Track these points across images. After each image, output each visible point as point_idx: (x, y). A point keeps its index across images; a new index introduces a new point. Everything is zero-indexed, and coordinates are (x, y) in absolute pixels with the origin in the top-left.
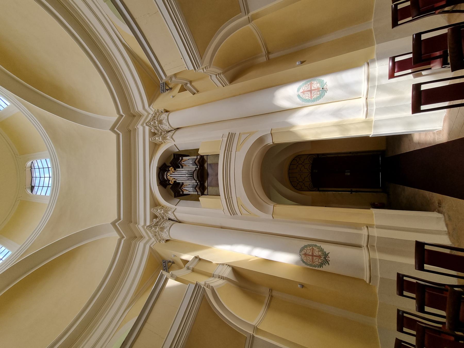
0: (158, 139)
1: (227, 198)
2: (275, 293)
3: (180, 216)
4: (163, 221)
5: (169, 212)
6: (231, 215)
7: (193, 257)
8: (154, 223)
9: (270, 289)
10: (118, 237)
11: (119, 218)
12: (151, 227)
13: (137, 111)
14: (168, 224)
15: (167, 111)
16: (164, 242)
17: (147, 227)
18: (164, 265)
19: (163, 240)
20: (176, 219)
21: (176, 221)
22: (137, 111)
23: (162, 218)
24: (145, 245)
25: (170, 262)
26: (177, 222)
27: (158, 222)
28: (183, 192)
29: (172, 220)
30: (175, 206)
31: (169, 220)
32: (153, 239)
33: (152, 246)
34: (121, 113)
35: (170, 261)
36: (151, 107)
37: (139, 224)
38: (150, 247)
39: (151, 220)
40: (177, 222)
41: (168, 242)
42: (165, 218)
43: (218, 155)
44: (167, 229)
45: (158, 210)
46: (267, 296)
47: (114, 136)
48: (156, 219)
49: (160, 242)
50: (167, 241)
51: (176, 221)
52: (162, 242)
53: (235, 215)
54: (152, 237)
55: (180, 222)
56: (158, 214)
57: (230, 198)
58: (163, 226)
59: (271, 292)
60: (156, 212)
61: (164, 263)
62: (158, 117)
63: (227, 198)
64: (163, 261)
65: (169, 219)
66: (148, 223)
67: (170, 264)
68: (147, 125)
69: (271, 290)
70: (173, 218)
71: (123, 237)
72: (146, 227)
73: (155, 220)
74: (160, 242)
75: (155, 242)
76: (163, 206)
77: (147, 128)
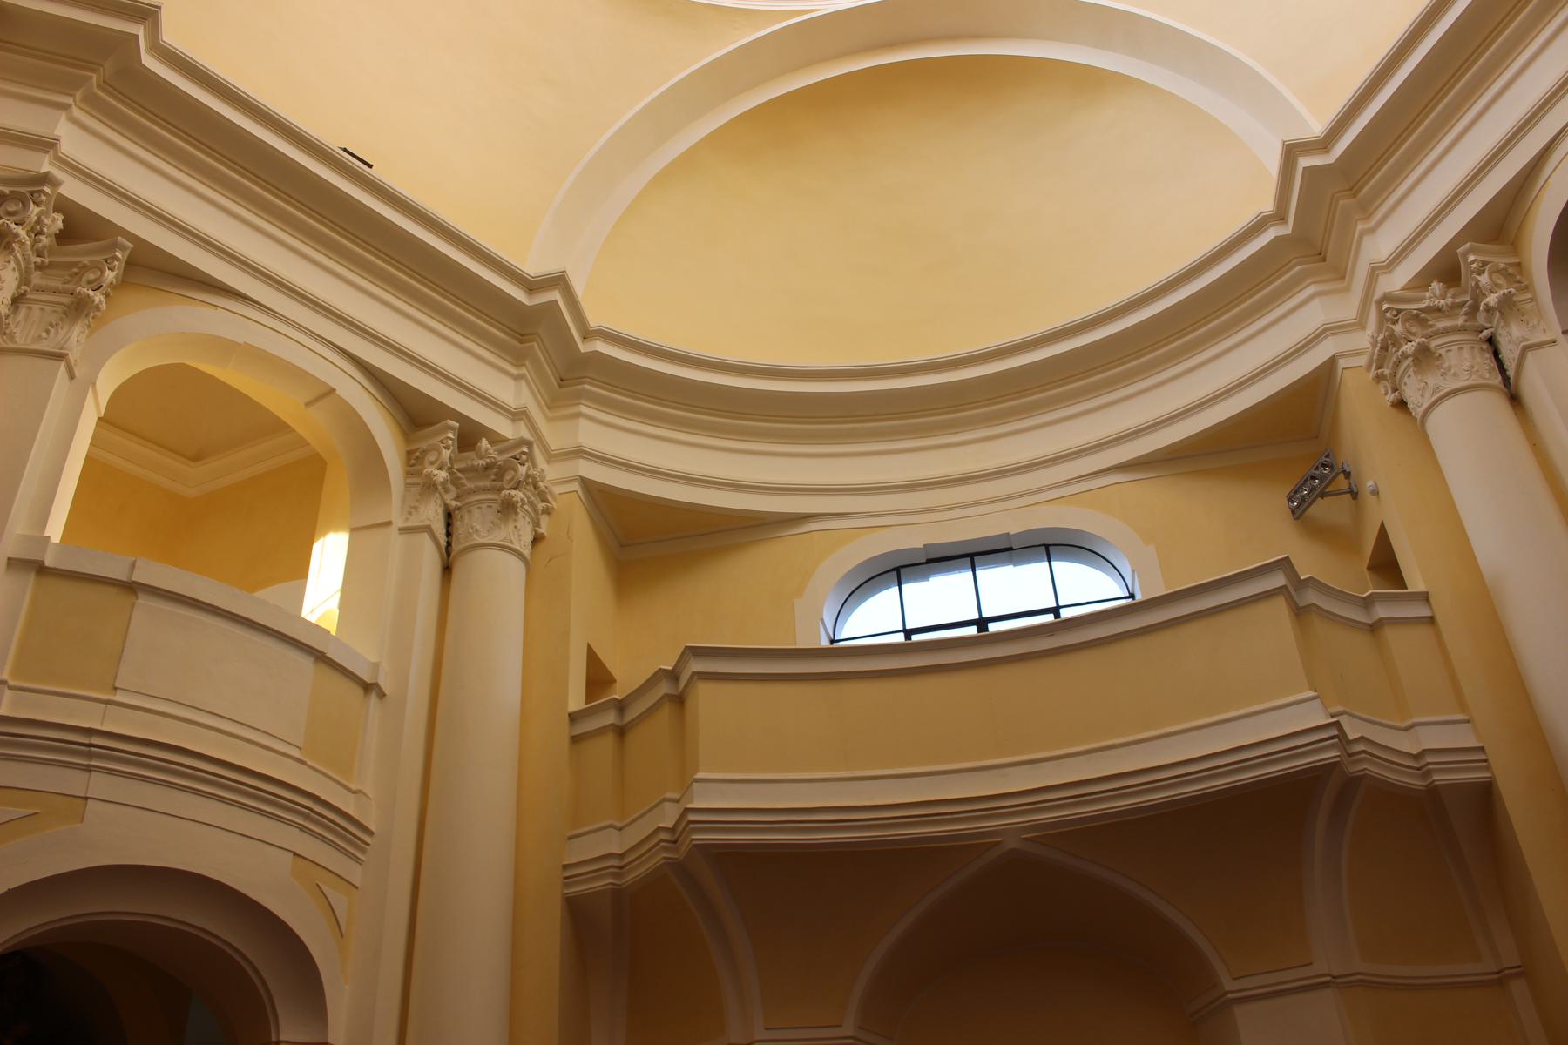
2: (1518, 988)
4: (1462, 326)
7: (1426, 590)
8: (1420, 300)
9: (1520, 967)
10: (1267, 205)
12: (1399, 311)
16: (1391, 397)
17: (1386, 298)
19: (1395, 390)
20: (1511, 373)
23: (1469, 307)
24: (1325, 330)
25: (1348, 475)
27: (1438, 309)
31: (1485, 346)
32: (1364, 339)
33: (1342, 363)
35: (1350, 472)
37: (1373, 230)
38: (1331, 364)
39: (1422, 281)
42: (1481, 318)
45: (1486, 274)
48: (1448, 288)
49: (1379, 378)
50: (1401, 404)
51: (1506, 379)
52: (1383, 392)
55: (1515, 399)
56: (1467, 280)
58: (1442, 351)
59: (1517, 975)
64: (1328, 456)
65: (1491, 340)
67: (1342, 483)
70: (1509, 354)
73: (1438, 293)
74: (1379, 378)
75: (1362, 361)
76: (1519, 264)
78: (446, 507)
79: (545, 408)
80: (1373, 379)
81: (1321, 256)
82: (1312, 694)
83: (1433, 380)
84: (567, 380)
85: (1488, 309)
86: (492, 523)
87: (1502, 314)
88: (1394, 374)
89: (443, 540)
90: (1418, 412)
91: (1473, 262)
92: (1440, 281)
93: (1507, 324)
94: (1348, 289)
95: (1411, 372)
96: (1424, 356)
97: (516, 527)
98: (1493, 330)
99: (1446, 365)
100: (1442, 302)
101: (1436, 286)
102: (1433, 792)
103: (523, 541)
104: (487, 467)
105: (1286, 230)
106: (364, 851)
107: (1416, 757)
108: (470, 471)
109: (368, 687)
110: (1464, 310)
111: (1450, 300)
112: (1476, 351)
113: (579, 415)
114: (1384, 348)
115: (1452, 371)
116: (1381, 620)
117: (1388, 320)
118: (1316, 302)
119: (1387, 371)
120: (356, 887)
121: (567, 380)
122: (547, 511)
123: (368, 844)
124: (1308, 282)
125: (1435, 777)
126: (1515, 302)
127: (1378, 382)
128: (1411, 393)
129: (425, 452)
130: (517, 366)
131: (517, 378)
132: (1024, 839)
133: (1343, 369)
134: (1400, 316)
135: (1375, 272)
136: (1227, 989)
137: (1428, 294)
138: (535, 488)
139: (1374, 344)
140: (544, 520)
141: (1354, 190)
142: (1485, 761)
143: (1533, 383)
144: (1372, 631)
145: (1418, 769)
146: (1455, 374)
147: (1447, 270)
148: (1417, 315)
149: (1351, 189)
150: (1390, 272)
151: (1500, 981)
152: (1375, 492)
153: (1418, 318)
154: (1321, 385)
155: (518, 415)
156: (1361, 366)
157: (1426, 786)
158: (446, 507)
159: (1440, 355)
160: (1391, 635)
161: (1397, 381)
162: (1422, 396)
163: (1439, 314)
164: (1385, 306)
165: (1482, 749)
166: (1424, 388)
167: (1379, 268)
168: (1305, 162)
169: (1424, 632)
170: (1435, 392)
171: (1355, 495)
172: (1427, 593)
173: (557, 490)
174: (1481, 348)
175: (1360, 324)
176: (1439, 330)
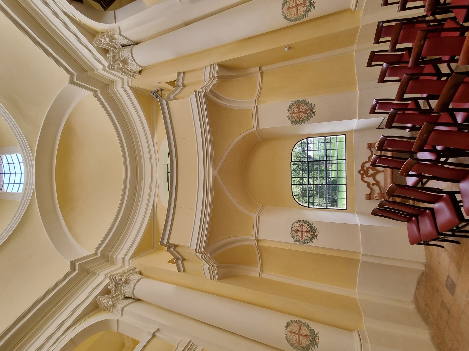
3: (133, 35)
4: (118, 51)
5: (116, 36)
7: (177, 73)
8: (111, 60)
10: (92, 93)
11: (71, 74)
12: (112, 65)
14: (126, 53)
16: (138, 75)
17: (108, 67)
18: (155, 96)
20: (130, 43)
21: (132, 45)
24: (123, 88)
25: (158, 91)
26: (134, 44)
27: (114, 56)
29: (127, 46)
30: (116, 23)
31: (124, 48)
32: (126, 78)
33: (130, 85)
38: (130, 87)
39: (106, 58)
40: (134, 44)
41: (143, 73)
42: (117, 47)
44: (130, 59)
48: (109, 53)
49: (134, 77)
50: (140, 72)
51: (132, 45)
54: (122, 75)
55: (137, 44)
56: (106, 47)
58: (123, 57)
60: (101, 43)
61: (153, 94)
65: (123, 46)
66: (106, 64)
67: (159, 92)
70: (125, 42)
71: (96, 91)
72: (107, 69)
73: (109, 55)
74: (134, 77)
75: (130, 80)
78: (123, 299)
79: (113, 265)
83: (130, 61)
84: (107, 259)
85: (111, 41)
86: (129, 287)
87: (113, 39)
89: (130, 301)
90: (140, 69)
91: (98, 42)
93: (115, 39)
94: (116, 81)
95: (129, 67)
96: (125, 62)
97: (132, 280)
100: (112, 55)
101: (108, 55)
102: (219, 77)
103: (138, 276)
104: (115, 287)
106: (195, 344)
107: (211, 79)
108: (116, 291)
109: (154, 336)
111: (112, 53)
112: (124, 49)
113: (116, 258)
114: (124, 72)
115: (128, 56)
116: (182, 83)
117: (114, 68)
118: (117, 88)
120: (203, 349)
121: (107, 259)
122: (135, 269)
123: (193, 342)
124: (113, 89)
125: (215, 76)
126: (111, 35)
127: (135, 77)
128: (135, 68)
129: (104, 306)
130: (96, 274)
131: (98, 275)
132: (215, 170)
136: (255, 129)
137: (110, 58)
138: (126, 273)
139: (124, 75)
140: (136, 271)
141: (86, 71)
142: (214, 65)
144: (185, 86)
145: (213, 79)
146: (128, 55)
147: (105, 51)
148: (114, 61)
149: (86, 72)
152: (159, 83)
153: (115, 61)
154: (138, 92)
155: (106, 276)
157: (217, 78)
158: (123, 299)
159: (124, 58)
160: (185, 82)
162: (134, 65)
165: (211, 65)
166: (132, 64)
167: (104, 68)
169: (186, 75)
171: (162, 90)
173: (131, 266)
174: (125, 48)
176: (118, 57)
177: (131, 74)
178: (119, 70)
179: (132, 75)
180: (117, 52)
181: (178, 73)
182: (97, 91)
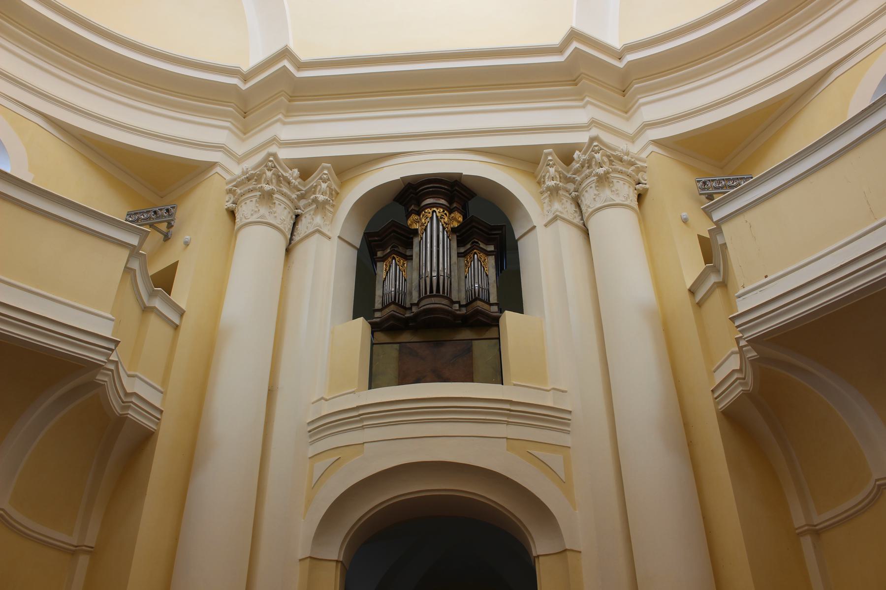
0: (552, 172)
1: (361, 412)
2: (83, 561)
3: (307, 251)
4: (293, 199)
5: (318, 219)
6: (309, 424)
7: (185, 310)
8: (286, 171)
9: (92, 548)
10: (245, 68)
12: (275, 167)
13: (641, 101)
14: (282, 215)
15: (640, 197)
16: (230, 205)
17: (274, 155)
18: (161, 210)
19: (234, 203)
20: (297, 238)
21: (291, 239)
22: (638, 100)
23: (301, 194)
25: (170, 226)
26: (290, 243)
27: (289, 183)
28: (383, 259)
29: (295, 224)
30: (339, 237)
31: (294, 217)
32: (237, 170)
33: (218, 169)
34: (630, 57)
35: (173, 226)
36: (652, 148)
37: (285, 123)
38: (212, 165)
39: (293, 163)
40: (290, 243)
41: (226, 218)
42: (302, 203)
43: (498, 377)
44: (267, 214)
45: (326, 185)
46: (74, 540)
47: (556, 39)
49: (230, 191)
50: (232, 213)
51: (291, 239)
52: (227, 200)
53: (311, 437)
54: (245, 169)
55: (288, 251)
56: (312, 181)
57: (362, 420)
58: (277, 202)
60: (321, 178)
61: (168, 210)
62: (621, 172)
63: (361, 412)
64: (173, 208)
65: (297, 216)
66: (284, 154)
67: (163, 227)
68: (592, 140)
69: (92, 552)
70: (303, 227)
73: (295, 175)
74: (230, 191)
75: (228, 177)
76: (337, 194)
77: (582, 138)
80: (226, 190)
81: (245, 114)
82: (110, 316)
83: (263, 211)
85: (315, 201)
87: (317, 208)
88: (242, 195)
92: (299, 171)
93: (315, 213)
94: (243, 140)
95: (254, 200)
96: (267, 197)
98: (303, 213)
99: (274, 210)
100: (294, 181)
101: (296, 172)
102: (123, 420)
105: (244, 87)
107: (127, 394)
110: (298, 193)
111: (297, 183)
114: (249, 179)
115: (275, 215)
116: (155, 308)
117: (266, 166)
118: (226, 132)
119: (239, 191)
124: (230, 120)
125: (130, 412)
126: (325, 208)
127: (228, 193)
128: (246, 211)
133: (217, 172)
134: (274, 169)
135: (274, 140)
137: (290, 172)
139: (244, 173)
141: (292, 98)
142: (159, 419)
143: (299, 252)
144: (143, 311)
145: (123, 402)
146: (276, 217)
147: (306, 169)
148: (279, 176)
149: (291, 97)
150: (279, 147)
151: (74, 552)
152: (187, 244)
153: (279, 178)
156: (225, 179)
157: (121, 415)
159: (275, 203)
160: (153, 319)
161: (240, 201)
162: (252, 215)
163: (287, 185)
164: (271, 159)
165: (161, 412)
166: (256, 212)
167: (277, 141)
168: (286, 63)
169: (169, 331)
170: (262, 217)
171: (167, 237)
172: (184, 312)
174: (292, 217)
175: (240, 160)
176: (283, 191)
177: (239, 191)
178: (257, 171)
179: (235, 190)
180: (294, 196)
181: (184, 312)
182: (245, 83)
